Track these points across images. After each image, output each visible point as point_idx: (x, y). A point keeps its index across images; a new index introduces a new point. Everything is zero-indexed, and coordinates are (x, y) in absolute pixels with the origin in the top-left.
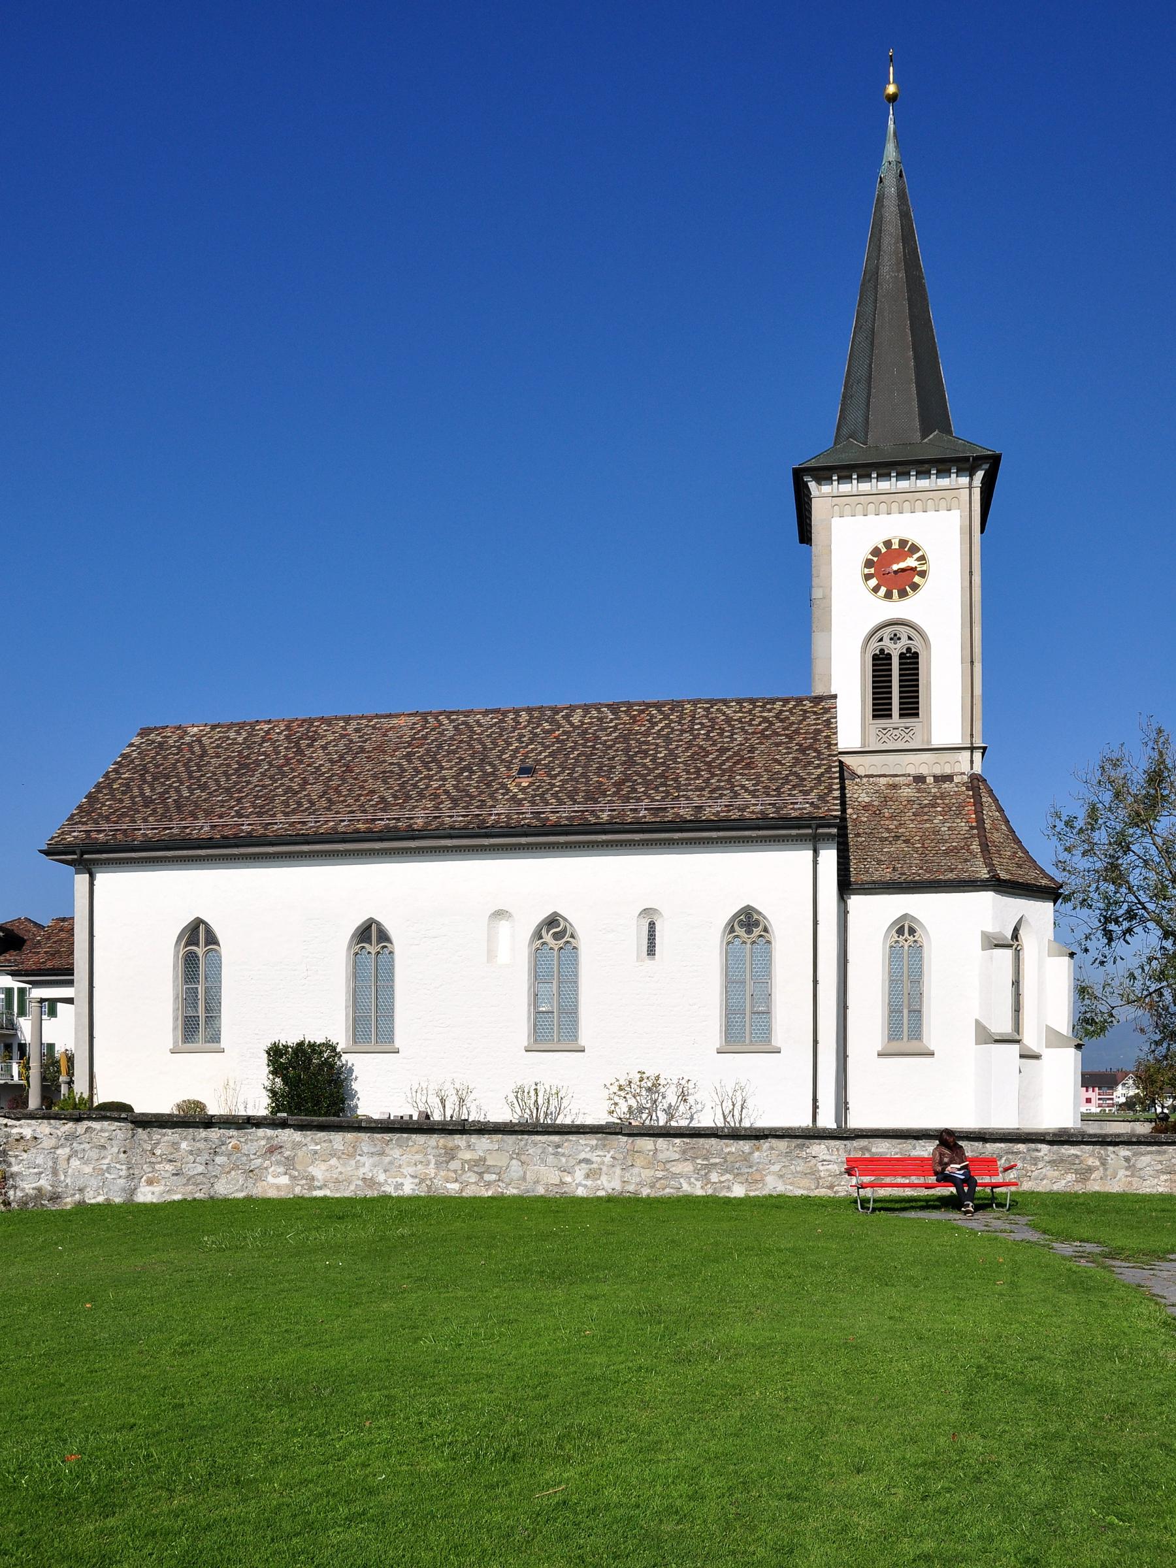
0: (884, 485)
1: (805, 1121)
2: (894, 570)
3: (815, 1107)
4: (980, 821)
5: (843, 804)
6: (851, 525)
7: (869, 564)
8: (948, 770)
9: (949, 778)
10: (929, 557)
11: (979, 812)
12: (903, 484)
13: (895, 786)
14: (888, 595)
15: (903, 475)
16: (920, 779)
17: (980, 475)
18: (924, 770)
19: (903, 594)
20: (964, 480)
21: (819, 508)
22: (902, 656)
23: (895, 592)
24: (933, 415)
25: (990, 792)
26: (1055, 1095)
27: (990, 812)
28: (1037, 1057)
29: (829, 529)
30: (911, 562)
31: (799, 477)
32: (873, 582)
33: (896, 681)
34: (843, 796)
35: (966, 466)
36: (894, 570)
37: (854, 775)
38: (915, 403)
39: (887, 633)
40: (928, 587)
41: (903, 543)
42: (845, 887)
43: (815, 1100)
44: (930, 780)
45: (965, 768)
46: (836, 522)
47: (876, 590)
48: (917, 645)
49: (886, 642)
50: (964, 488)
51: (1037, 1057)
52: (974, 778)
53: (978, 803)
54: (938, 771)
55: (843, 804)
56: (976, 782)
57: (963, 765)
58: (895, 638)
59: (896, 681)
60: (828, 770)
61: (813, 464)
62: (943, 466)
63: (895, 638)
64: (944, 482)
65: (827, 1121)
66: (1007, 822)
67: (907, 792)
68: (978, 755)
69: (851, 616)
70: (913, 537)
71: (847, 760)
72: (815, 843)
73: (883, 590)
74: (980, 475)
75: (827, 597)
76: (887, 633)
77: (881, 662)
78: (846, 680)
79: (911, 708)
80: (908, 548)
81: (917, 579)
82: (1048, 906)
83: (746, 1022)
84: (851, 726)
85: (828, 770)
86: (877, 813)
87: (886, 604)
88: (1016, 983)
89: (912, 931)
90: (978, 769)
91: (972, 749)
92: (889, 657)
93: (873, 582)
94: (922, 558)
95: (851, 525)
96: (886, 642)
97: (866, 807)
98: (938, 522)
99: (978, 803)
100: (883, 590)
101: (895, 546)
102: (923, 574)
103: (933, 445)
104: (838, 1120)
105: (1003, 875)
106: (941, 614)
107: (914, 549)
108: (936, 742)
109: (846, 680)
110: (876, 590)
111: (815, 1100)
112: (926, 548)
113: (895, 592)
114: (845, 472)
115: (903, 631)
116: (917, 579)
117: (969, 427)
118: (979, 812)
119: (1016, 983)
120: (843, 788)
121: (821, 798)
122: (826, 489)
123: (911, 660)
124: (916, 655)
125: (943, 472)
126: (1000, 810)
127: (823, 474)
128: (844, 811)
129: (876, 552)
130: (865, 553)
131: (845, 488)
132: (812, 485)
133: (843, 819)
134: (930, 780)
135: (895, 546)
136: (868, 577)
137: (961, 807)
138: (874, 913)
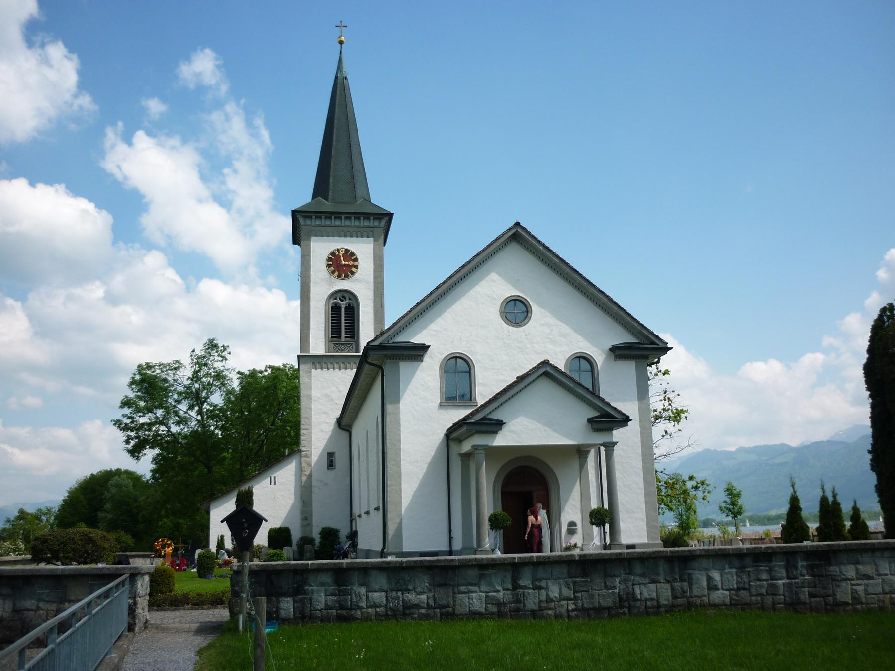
2: (341, 264)
14: (339, 276)
19: (346, 277)
23: (343, 275)
32: (332, 269)
36: (341, 264)
39: (339, 295)
40: (359, 273)
47: (333, 273)
73: (336, 273)
76: (339, 295)
77: (335, 309)
80: (349, 255)
92: (340, 308)
93: (332, 269)
110: (333, 273)
112: (358, 255)
113: (343, 275)
115: (347, 296)
122: (308, 222)
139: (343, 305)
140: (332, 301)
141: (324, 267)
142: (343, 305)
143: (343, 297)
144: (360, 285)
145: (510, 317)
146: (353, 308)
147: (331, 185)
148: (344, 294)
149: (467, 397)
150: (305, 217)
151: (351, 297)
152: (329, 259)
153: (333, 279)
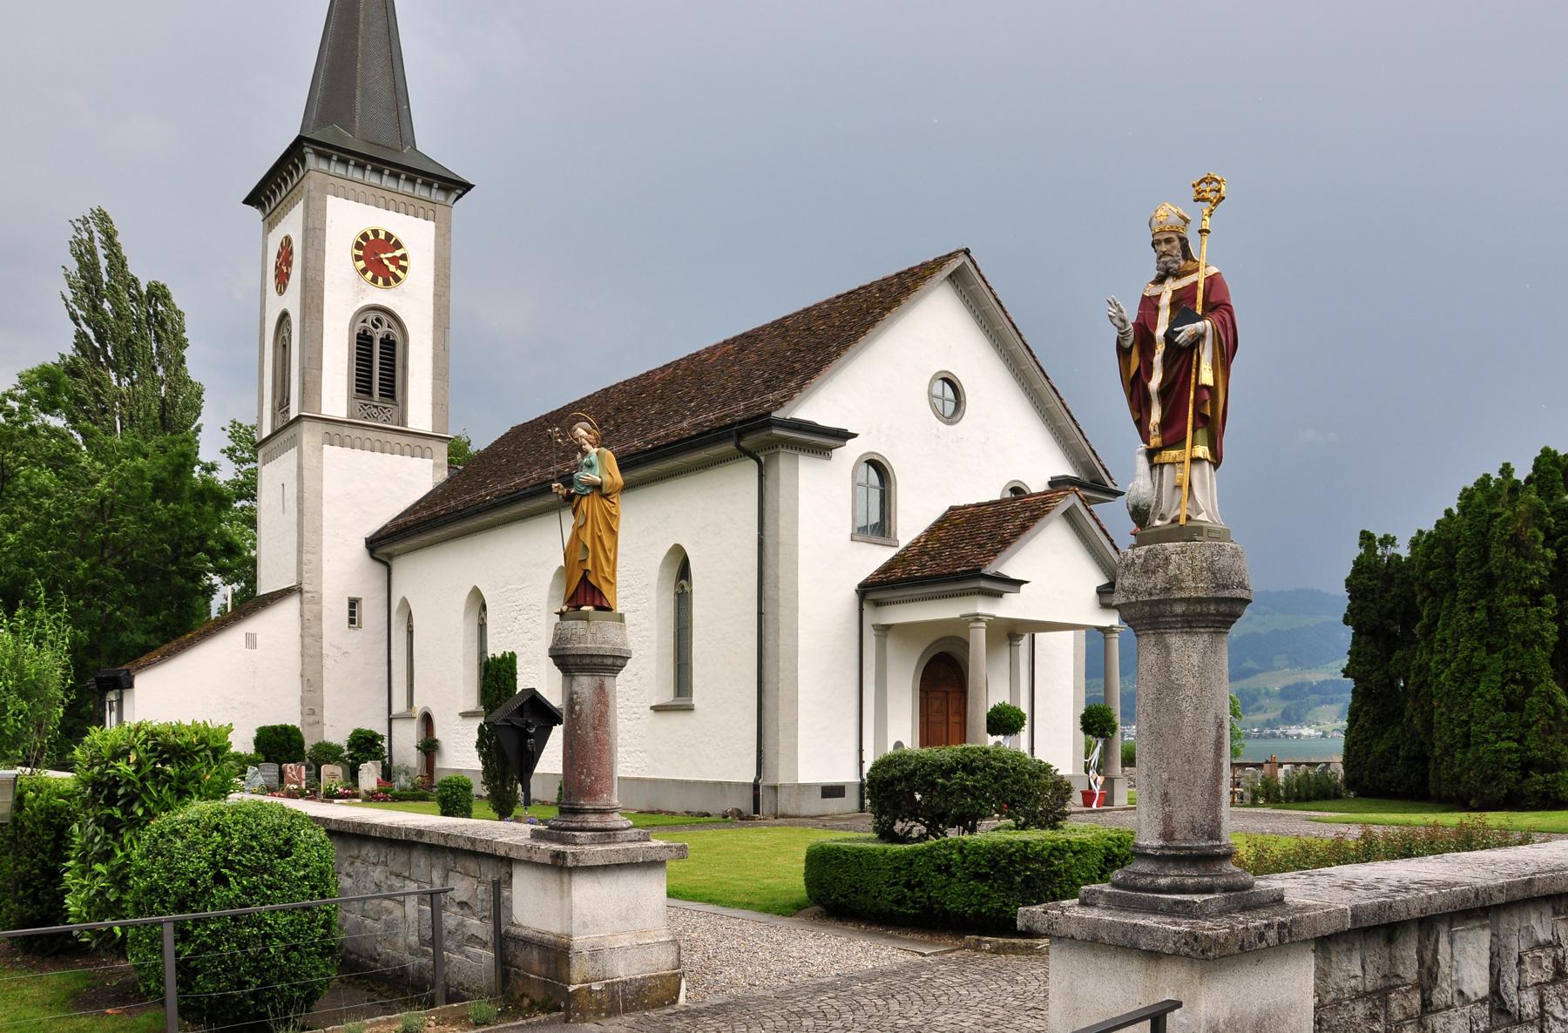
19: (387, 283)
22: (382, 341)
23: (380, 280)
32: (362, 264)
36: (378, 256)
40: (408, 279)
41: (389, 236)
47: (364, 271)
70: (398, 234)
73: (370, 275)
76: (372, 316)
87: (371, 288)
101: (382, 236)
112: (408, 248)
113: (380, 280)
123: (388, 344)
129: (364, 236)
130: (354, 236)
132: (311, 159)
139: (379, 334)
140: (360, 325)
141: (349, 259)
142: (379, 334)
143: (378, 320)
144: (412, 301)
145: (939, 403)
146: (393, 343)
147: (358, 106)
148: (384, 317)
149: (881, 529)
150: (319, 155)
151: (393, 323)
152: (358, 246)
153: (364, 283)
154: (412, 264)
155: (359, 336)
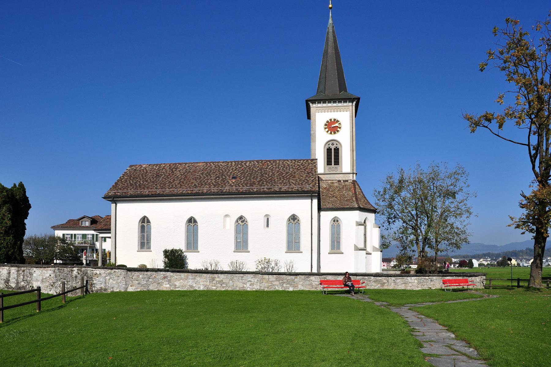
0: (330, 105)
1: (309, 271)
2: (332, 127)
3: (312, 267)
4: (355, 192)
5: (319, 187)
6: (321, 115)
7: (326, 125)
8: (347, 179)
9: (347, 181)
10: (342, 123)
11: (355, 190)
12: (335, 105)
13: (333, 183)
14: (331, 133)
15: (335, 102)
16: (339, 181)
17: (355, 103)
18: (340, 179)
19: (335, 133)
20: (351, 104)
21: (312, 110)
22: (334, 149)
24: (342, 86)
25: (358, 185)
26: (375, 264)
27: (358, 190)
28: (370, 254)
29: (315, 115)
30: (337, 125)
31: (307, 102)
32: (327, 130)
33: (333, 155)
34: (319, 185)
35: (351, 100)
36: (332, 127)
37: (322, 180)
38: (337, 84)
39: (331, 143)
40: (341, 131)
41: (335, 120)
42: (320, 209)
43: (312, 265)
44: (342, 181)
45: (351, 178)
46: (317, 114)
47: (328, 132)
48: (339, 146)
49: (330, 145)
50: (350, 106)
51: (370, 254)
52: (353, 181)
53: (355, 188)
54: (344, 179)
55: (319, 187)
56: (354, 182)
57: (351, 178)
58: (333, 144)
59: (333, 155)
60: (315, 178)
61: (311, 99)
62: (345, 100)
63: (333, 144)
64: (345, 104)
65: (315, 270)
66: (362, 193)
67: (336, 184)
68: (355, 175)
69: (321, 139)
71: (320, 176)
72: (312, 198)
73: (329, 132)
74: (355, 103)
75: (315, 133)
77: (329, 150)
78: (320, 155)
79: (337, 162)
81: (338, 129)
82: (373, 215)
83: (293, 245)
84: (321, 167)
85: (315, 178)
86: (328, 190)
88: (365, 235)
89: (337, 221)
90: (355, 179)
91: (353, 173)
92: (331, 149)
93: (327, 130)
94: (340, 124)
95: (321, 115)
96: (330, 145)
97: (325, 188)
98: (344, 115)
99: (355, 188)
100: (329, 132)
102: (340, 128)
103: (342, 95)
104: (318, 270)
105: (362, 207)
106: (345, 138)
107: (338, 121)
108: (344, 171)
109: (320, 155)
110: (328, 132)
111: (312, 265)
112: (341, 121)
114: (319, 101)
116: (338, 129)
117: (352, 91)
118: (355, 190)
119: (365, 235)
120: (319, 183)
121: (313, 186)
122: (314, 105)
123: (337, 150)
124: (338, 149)
125: (345, 102)
126: (361, 189)
127: (314, 102)
128: (319, 189)
129: (328, 122)
131: (319, 105)
132: (311, 104)
133: (319, 191)
134: (342, 181)
135: (333, 120)
136: (325, 128)
137: (350, 188)
138: (327, 216)
139: (333, 148)
140: (327, 147)
142: (333, 148)
150: (312, 103)
154: (343, 126)
155: (327, 149)
